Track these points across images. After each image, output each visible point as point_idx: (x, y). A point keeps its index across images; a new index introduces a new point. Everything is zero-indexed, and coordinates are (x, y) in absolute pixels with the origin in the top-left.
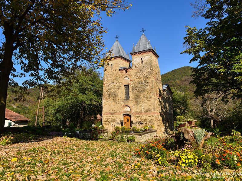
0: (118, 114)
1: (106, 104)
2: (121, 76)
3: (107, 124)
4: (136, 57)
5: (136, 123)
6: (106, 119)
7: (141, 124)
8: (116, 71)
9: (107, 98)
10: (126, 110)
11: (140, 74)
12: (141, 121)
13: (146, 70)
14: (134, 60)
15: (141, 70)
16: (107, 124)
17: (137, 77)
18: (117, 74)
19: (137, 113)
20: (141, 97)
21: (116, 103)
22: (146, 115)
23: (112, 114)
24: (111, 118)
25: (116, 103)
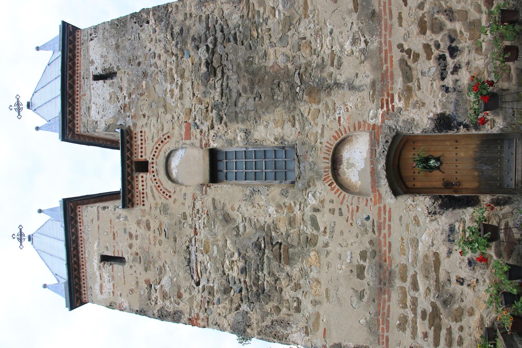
0: (385, 231)
1: (318, 315)
2: (161, 200)
3: (455, 327)
4: (83, 110)
5: (447, 90)
6: (420, 334)
7: (453, 51)
8: (133, 228)
9: (278, 310)
10: (361, 173)
11: (160, 77)
12: (436, 53)
13: (149, 46)
14: (97, 117)
15: (145, 74)
16: (455, 327)
17: (177, 91)
18: (148, 227)
19: (380, 89)
20: (281, 60)
21: (311, 241)
22: (395, 19)
23: (384, 280)
24: (415, 286)
25: (311, 241)
